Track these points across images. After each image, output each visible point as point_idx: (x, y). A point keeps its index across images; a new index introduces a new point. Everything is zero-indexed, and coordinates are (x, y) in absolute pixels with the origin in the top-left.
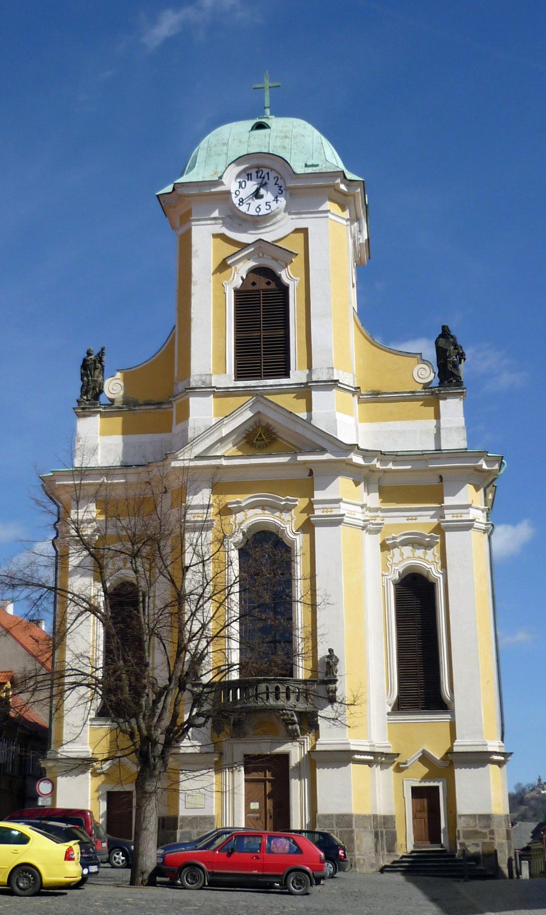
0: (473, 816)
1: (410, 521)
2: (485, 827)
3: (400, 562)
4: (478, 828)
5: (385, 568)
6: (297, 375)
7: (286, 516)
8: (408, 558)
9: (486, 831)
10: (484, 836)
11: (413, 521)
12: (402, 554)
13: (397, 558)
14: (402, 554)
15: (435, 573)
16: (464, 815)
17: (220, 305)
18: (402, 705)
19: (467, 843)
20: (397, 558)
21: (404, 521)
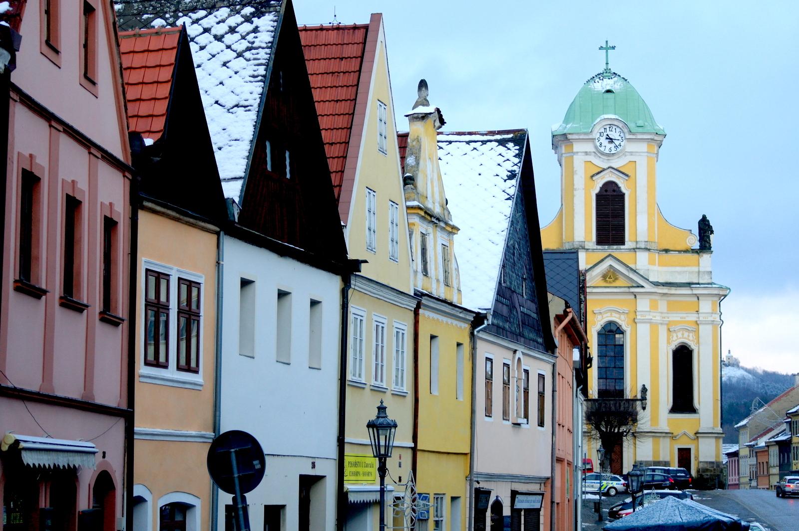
0: (706, 462)
1: (682, 319)
2: (712, 467)
3: (676, 340)
4: (708, 468)
5: (669, 342)
6: (629, 244)
7: (623, 317)
8: (680, 338)
9: (712, 469)
10: (711, 471)
11: (684, 319)
12: (677, 336)
13: (675, 338)
14: (677, 336)
15: (693, 346)
16: (702, 462)
17: (587, 205)
18: (674, 410)
19: (703, 474)
20: (675, 338)
21: (679, 319)
